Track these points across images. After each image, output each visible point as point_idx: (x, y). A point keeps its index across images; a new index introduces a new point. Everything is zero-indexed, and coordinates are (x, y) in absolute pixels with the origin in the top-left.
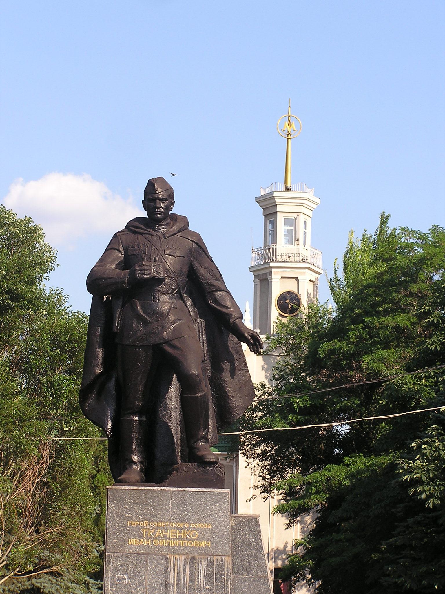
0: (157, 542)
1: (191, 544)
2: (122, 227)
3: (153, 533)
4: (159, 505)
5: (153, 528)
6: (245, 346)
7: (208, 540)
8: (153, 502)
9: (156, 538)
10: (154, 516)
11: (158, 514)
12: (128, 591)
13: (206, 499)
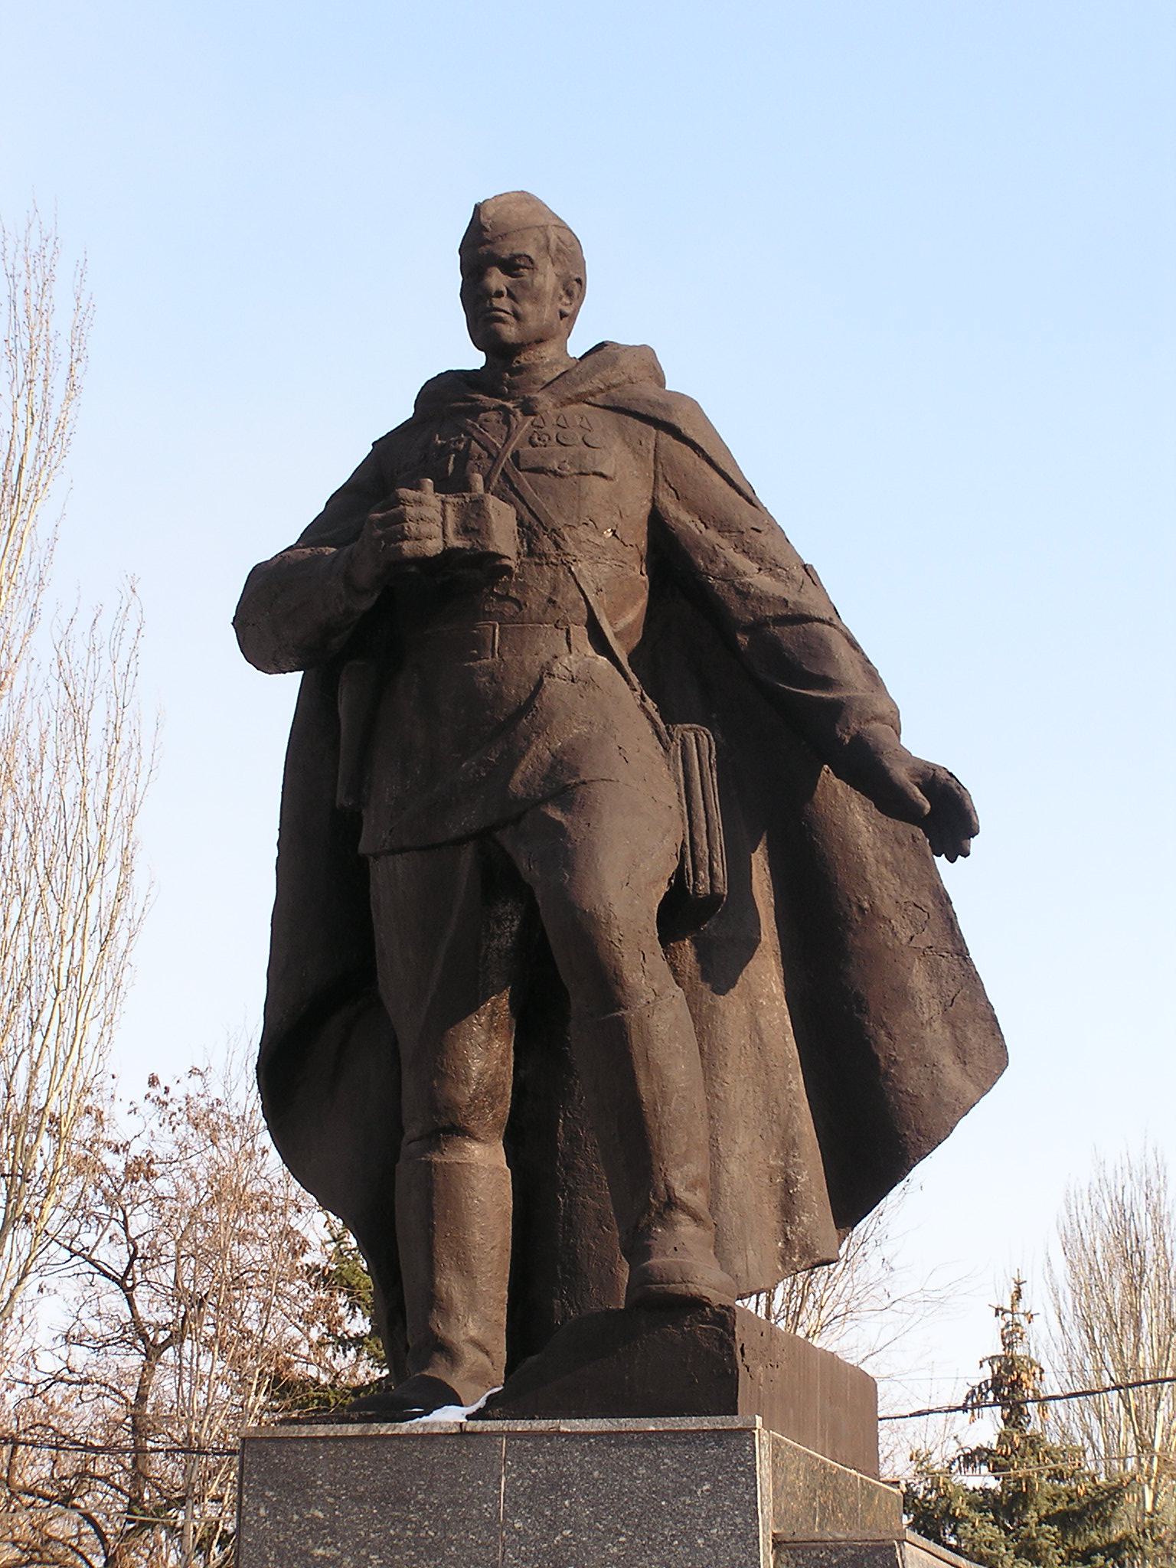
2: (404, 411)
4: (453, 1502)
8: (430, 1488)
13: (654, 1465)
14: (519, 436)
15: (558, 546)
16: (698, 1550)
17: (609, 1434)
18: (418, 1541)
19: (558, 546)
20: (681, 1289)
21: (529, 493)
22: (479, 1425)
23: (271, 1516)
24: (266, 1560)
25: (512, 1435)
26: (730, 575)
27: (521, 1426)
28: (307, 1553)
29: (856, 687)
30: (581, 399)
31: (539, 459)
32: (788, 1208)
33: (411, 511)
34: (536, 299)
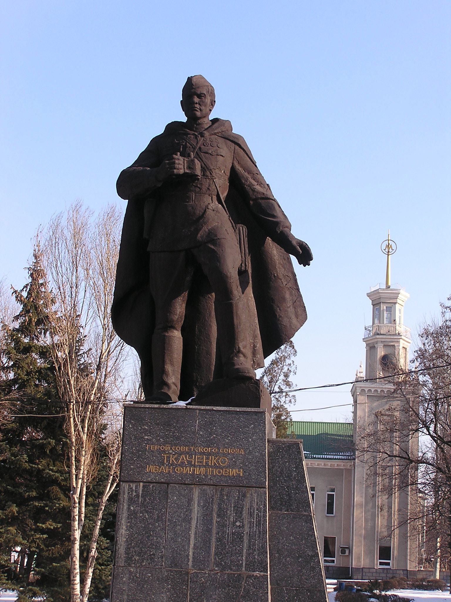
0: (179, 470)
1: (219, 472)
2: (161, 131)
3: (175, 459)
5: (176, 453)
6: (294, 259)
7: (240, 468)
9: (179, 465)
10: (178, 438)
11: (183, 437)
12: (144, 527)
13: (238, 420)
14: (200, 143)
15: (211, 174)
16: (250, 442)
17: (226, 411)
18: (174, 436)
19: (211, 174)
20: (248, 375)
21: (204, 159)
22: (189, 406)
23: (133, 427)
24: (131, 439)
25: (200, 410)
26: (251, 185)
27: (203, 407)
28: (143, 437)
29: (281, 218)
30: (215, 134)
31: (206, 150)
32: (254, 353)
33: (177, 161)
34: (205, 106)
